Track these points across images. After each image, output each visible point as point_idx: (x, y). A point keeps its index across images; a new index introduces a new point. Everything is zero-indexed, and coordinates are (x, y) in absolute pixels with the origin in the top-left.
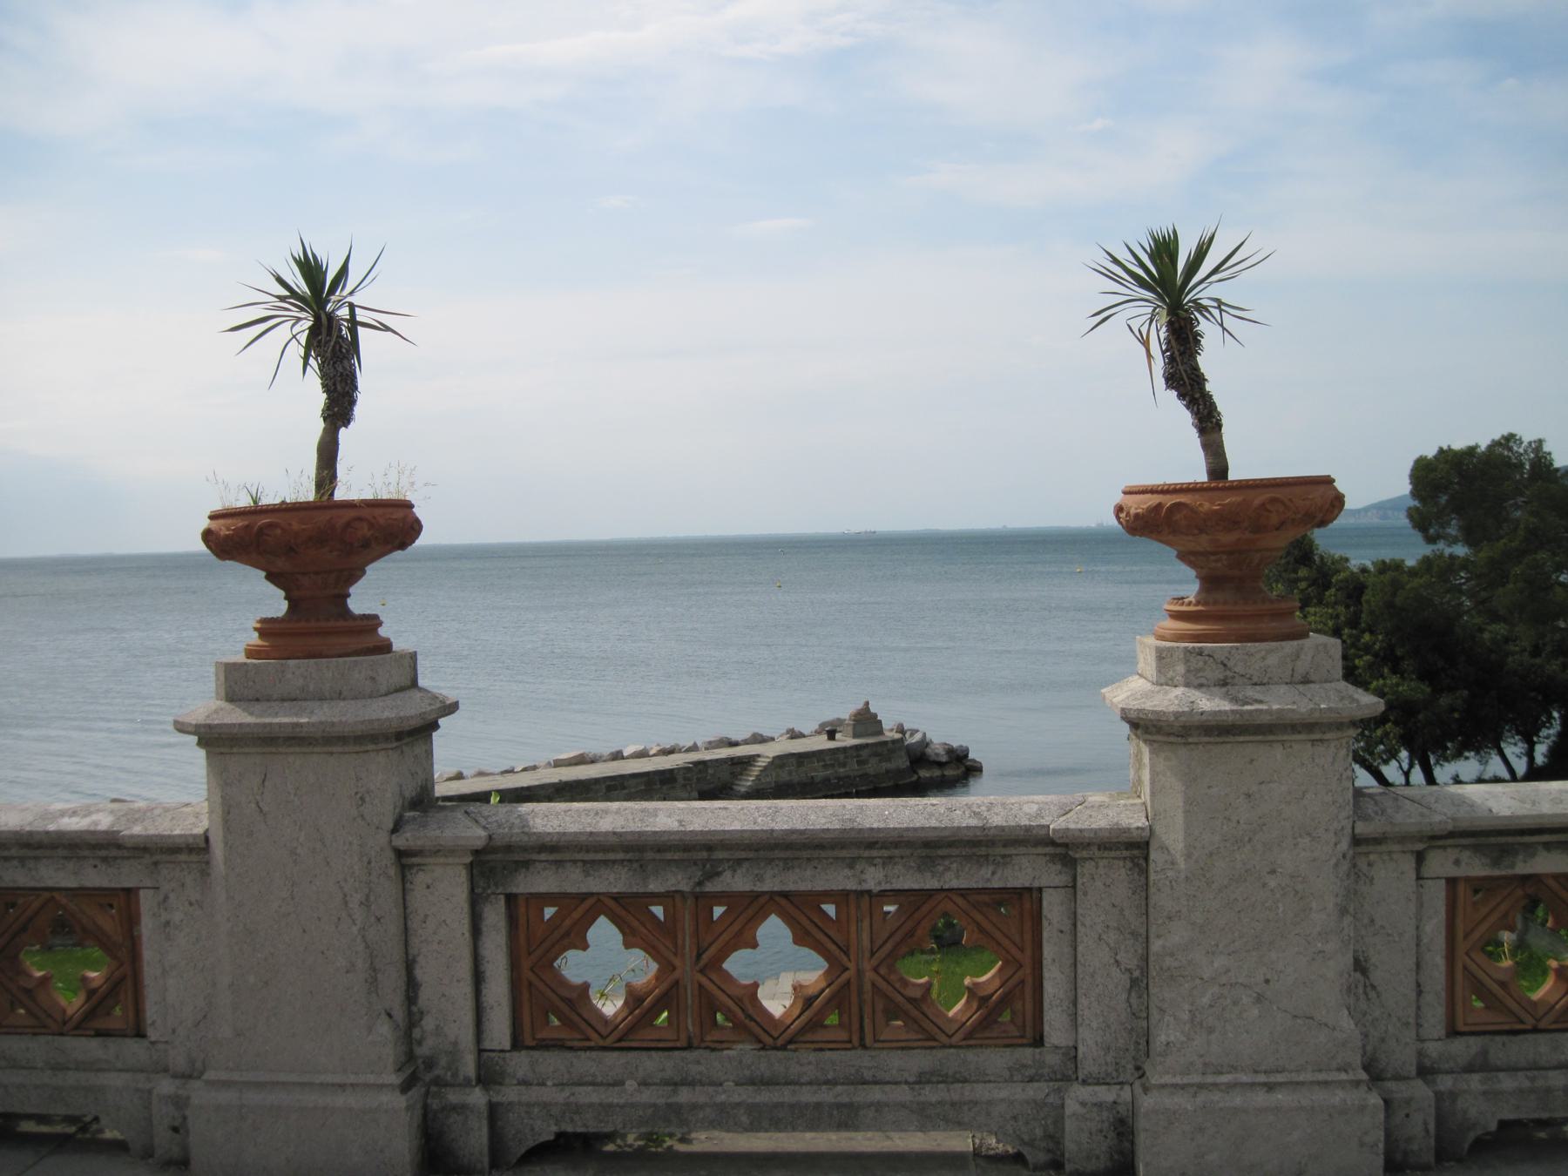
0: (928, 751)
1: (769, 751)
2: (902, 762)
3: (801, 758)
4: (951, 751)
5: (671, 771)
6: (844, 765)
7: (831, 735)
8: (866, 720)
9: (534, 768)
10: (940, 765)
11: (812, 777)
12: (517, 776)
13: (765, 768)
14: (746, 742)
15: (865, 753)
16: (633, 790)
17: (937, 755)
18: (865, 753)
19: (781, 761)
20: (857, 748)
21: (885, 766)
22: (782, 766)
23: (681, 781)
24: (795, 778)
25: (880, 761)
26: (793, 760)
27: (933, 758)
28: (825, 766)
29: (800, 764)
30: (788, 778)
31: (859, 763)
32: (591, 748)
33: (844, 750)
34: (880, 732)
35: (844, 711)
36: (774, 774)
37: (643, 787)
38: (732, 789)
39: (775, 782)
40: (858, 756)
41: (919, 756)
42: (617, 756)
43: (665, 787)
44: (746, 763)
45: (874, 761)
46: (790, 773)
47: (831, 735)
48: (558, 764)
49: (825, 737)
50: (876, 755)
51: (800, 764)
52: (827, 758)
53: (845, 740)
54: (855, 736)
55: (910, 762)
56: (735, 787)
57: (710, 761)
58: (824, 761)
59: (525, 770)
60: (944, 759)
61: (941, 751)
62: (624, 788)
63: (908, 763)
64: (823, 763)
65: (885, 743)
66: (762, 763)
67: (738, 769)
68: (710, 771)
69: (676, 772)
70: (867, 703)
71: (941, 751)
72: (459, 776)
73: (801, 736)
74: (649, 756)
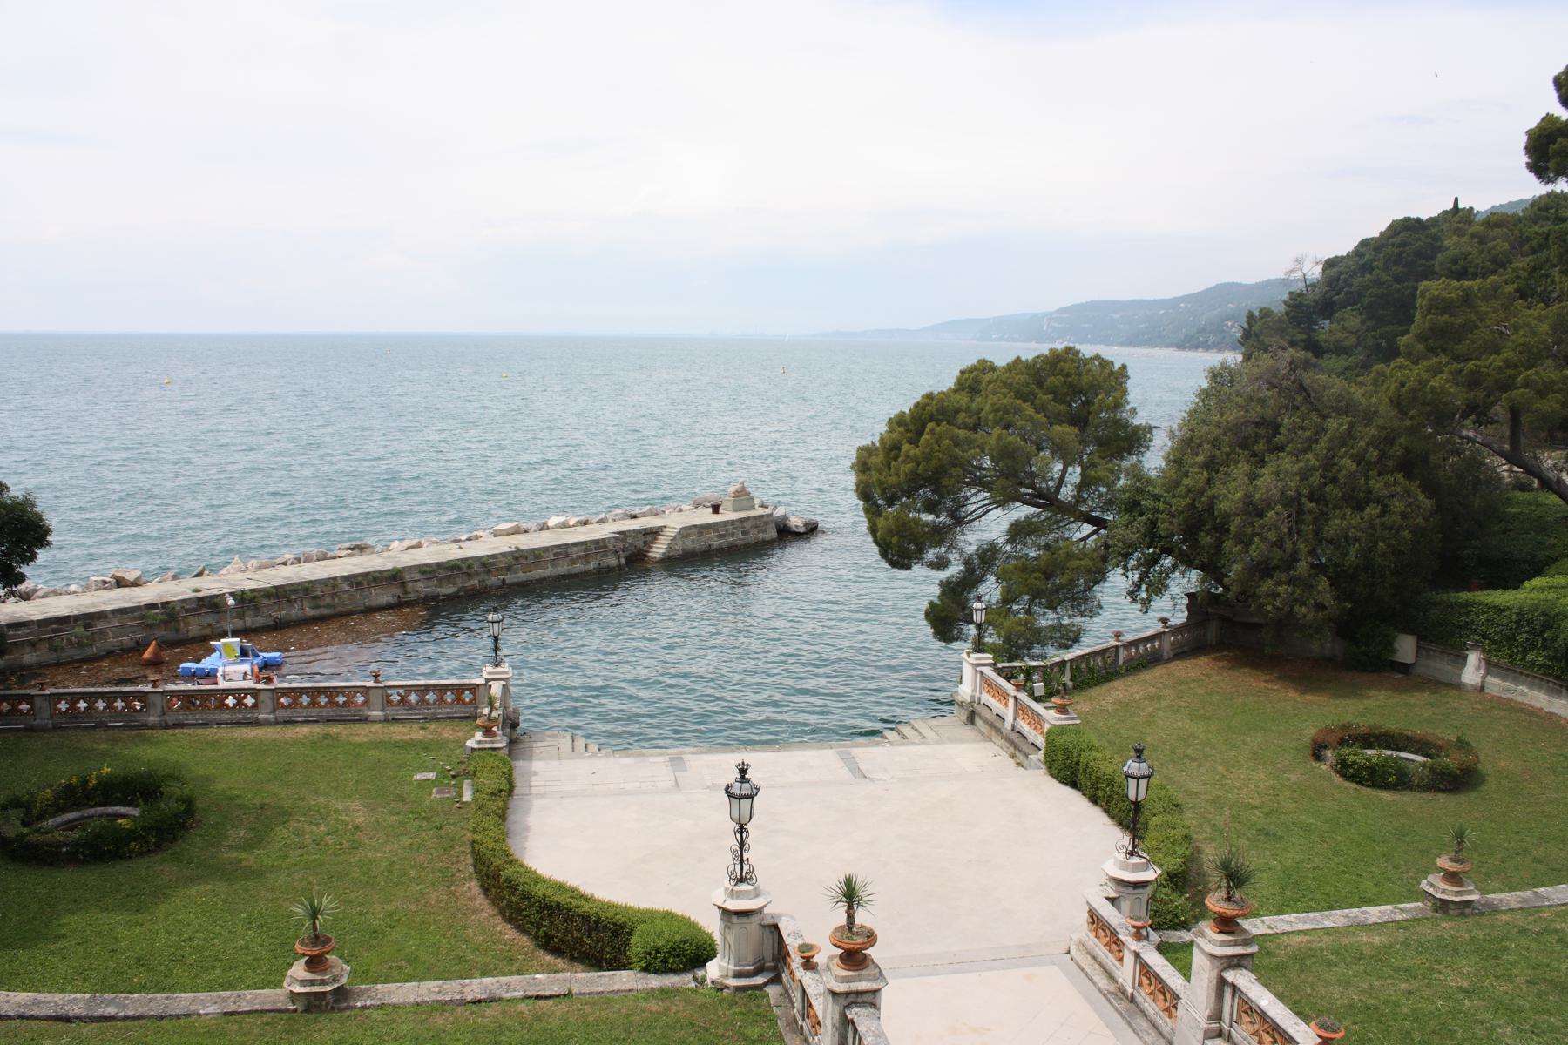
5: (604, 540)
6: (733, 535)
13: (674, 538)
17: (797, 526)
18: (748, 525)
19: (685, 532)
20: (742, 520)
22: (686, 536)
24: (697, 546)
25: (759, 532)
26: (695, 531)
28: (720, 536)
29: (700, 534)
31: (745, 533)
33: (725, 523)
38: (646, 556)
45: (755, 531)
46: (693, 541)
47: (716, 509)
49: (710, 510)
50: (756, 526)
51: (700, 534)
53: (726, 515)
54: (735, 511)
56: (650, 554)
57: (629, 531)
60: (802, 530)
67: (649, 538)
68: (629, 540)
74: (548, 528)
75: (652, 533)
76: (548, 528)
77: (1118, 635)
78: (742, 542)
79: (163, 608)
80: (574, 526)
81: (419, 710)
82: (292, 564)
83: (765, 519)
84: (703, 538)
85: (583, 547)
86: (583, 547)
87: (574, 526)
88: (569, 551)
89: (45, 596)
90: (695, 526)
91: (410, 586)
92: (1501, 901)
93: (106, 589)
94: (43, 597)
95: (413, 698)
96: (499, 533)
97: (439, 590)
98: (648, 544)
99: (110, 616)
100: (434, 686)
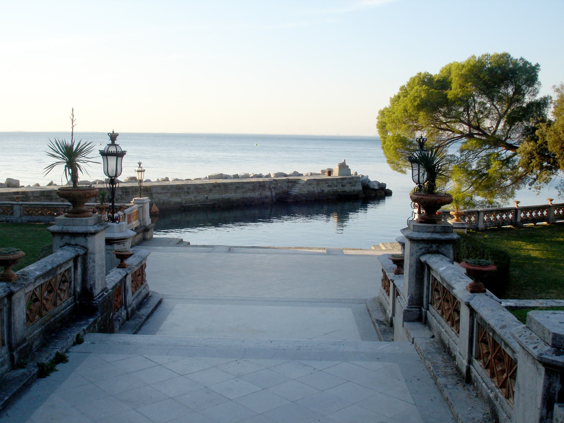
2: (359, 187)
4: (379, 184)
6: (337, 186)
11: (323, 190)
15: (345, 181)
18: (345, 181)
22: (310, 184)
25: (351, 186)
27: (372, 187)
28: (329, 186)
30: (313, 190)
31: (343, 186)
32: (225, 173)
39: (307, 191)
45: (348, 185)
46: (314, 187)
50: (350, 183)
51: (318, 184)
52: (329, 182)
55: (363, 188)
63: (362, 188)
64: (327, 185)
68: (279, 185)
69: (265, 183)
75: (292, 182)
76: (238, 177)
78: (341, 190)
79: (22, 194)
83: (355, 179)
88: (244, 186)
97: (171, 199)
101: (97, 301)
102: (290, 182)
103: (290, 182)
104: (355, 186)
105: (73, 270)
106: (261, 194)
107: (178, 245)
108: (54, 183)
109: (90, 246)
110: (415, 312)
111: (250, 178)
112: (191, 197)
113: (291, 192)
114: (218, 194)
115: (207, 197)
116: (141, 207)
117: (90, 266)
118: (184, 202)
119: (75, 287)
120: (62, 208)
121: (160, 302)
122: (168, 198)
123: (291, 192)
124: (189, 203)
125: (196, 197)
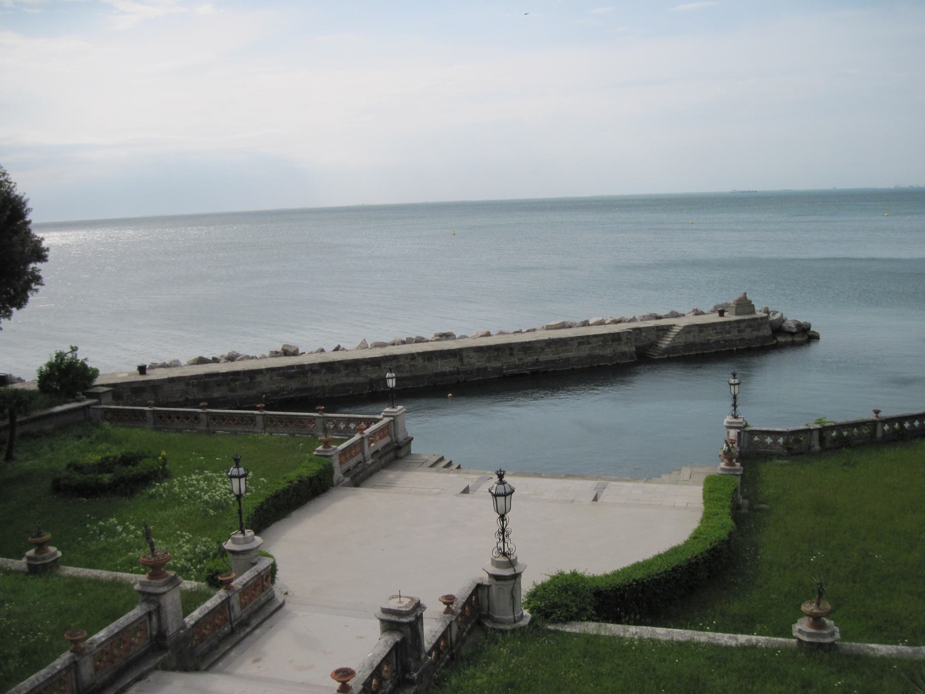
0: (784, 325)
1: (681, 323)
2: (767, 332)
3: (702, 327)
4: (799, 325)
5: (619, 334)
6: (729, 332)
7: (721, 313)
8: (744, 305)
9: (534, 330)
10: (792, 334)
11: (708, 340)
12: (523, 335)
13: (678, 333)
14: (667, 317)
16: (594, 345)
17: (790, 327)
18: (743, 325)
19: (688, 329)
20: (738, 322)
21: (756, 333)
22: (689, 333)
23: (624, 339)
24: (697, 340)
25: (753, 331)
27: (787, 329)
28: (717, 333)
31: (739, 331)
32: (569, 320)
33: (730, 323)
34: (753, 312)
35: (731, 298)
36: (684, 337)
37: (601, 343)
38: (657, 346)
39: (685, 342)
40: (738, 327)
41: (778, 328)
42: (585, 324)
43: (614, 344)
44: (666, 329)
45: (748, 330)
46: (694, 336)
47: (721, 313)
48: (549, 328)
49: (717, 314)
50: (750, 326)
52: (718, 328)
53: (730, 317)
54: (737, 314)
55: (773, 332)
56: (659, 345)
57: (644, 328)
58: (716, 329)
59: (528, 331)
60: (794, 330)
61: (793, 325)
62: (589, 343)
63: (771, 332)
64: (715, 331)
65: (756, 319)
66: (676, 330)
67: (661, 333)
68: (643, 334)
69: (621, 334)
70: (745, 294)
71: (793, 325)
72: (488, 334)
73: (702, 313)
74: (605, 324)
77: (877, 412)
80: (609, 324)
81: (345, 433)
82: (398, 344)
84: (702, 334)
85: (602, 338)
86: (602, 338)
87: (609, 324)
88: (590, 341)
89: (241, 359)
90: (697, 325)
91: (466, 361)
92: (873, 649)
93: (277, 357)
94: (239, 360)
95: (342, 426)
96: (549, 327)
97: (488, 364)
98: (659, 338)
99: (265, 372)
100: (354, 418)
101: (168, 643)
102: (660, 330)
103: (660, 330)
104: (759, 330)
105: (148, 620)
106: (614, 350)
107: (433, 469)
108: (342, 345)
109: (162, 602)
110: (398, 662)
111: (607, 324)
112: (515, 360)
113: (662, 344)
114: (553, 355)
115: (537, 359)
116: (391, 420)
117: (163, 615)
118: (506, 367)
119: (151, 632)
120: (307, 419)
121: (281, 606)
122: (484, 363)
123: (662, 344)
124: (513, 369)
125: (521, 359)
